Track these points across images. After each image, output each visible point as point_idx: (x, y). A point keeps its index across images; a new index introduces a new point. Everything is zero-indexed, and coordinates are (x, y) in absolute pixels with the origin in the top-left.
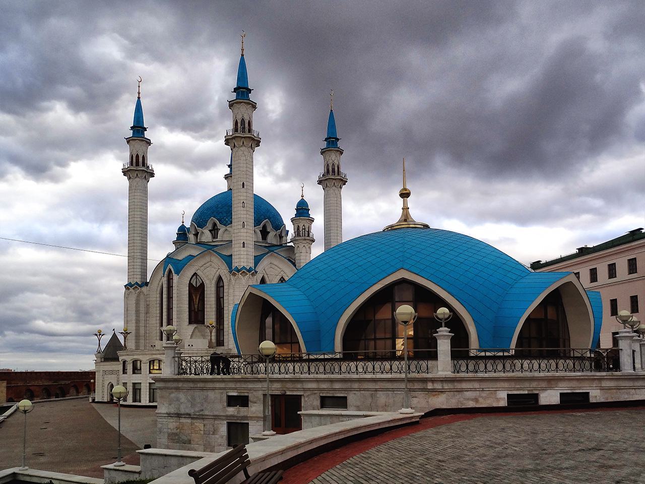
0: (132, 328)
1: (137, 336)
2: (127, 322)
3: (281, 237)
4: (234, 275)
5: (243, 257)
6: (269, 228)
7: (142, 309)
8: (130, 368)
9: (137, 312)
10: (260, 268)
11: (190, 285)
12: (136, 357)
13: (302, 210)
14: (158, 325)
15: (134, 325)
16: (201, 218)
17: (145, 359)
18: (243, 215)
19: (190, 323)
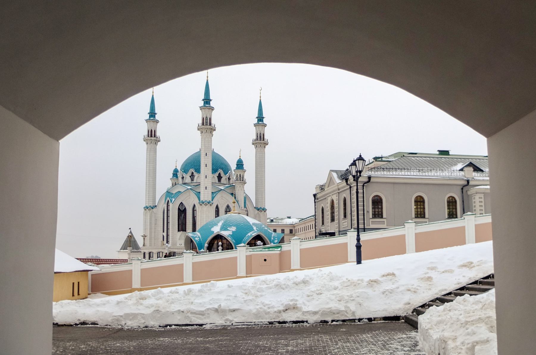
0: (148, 234)
1: (150, 239)
2: (145, 229)
3: (229, 179)
4: (201, 205)
5: (206, 195)
6: (222, 175)
7: (153, 222)
8: (147, 256)
9: (150, 223)
10: (214, 201)
11: (179, 209)
12: (150, 251)
13: (240, 165)
14: (162, 231)
15: (148, 231)
16: (185, 169)
17: (155, 251)
18: (206, 169)
19: (179, 231)
